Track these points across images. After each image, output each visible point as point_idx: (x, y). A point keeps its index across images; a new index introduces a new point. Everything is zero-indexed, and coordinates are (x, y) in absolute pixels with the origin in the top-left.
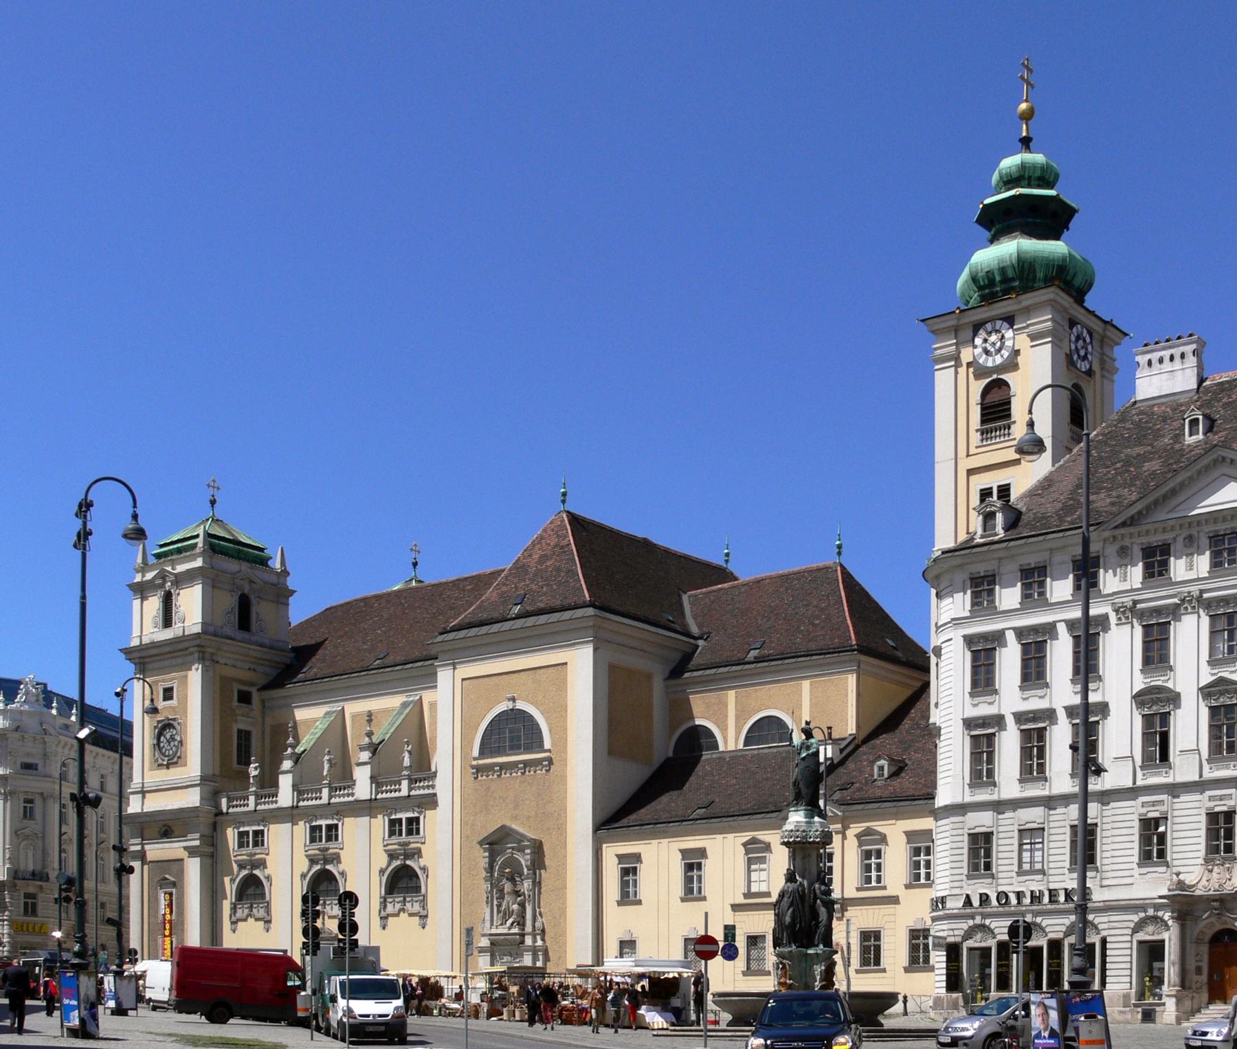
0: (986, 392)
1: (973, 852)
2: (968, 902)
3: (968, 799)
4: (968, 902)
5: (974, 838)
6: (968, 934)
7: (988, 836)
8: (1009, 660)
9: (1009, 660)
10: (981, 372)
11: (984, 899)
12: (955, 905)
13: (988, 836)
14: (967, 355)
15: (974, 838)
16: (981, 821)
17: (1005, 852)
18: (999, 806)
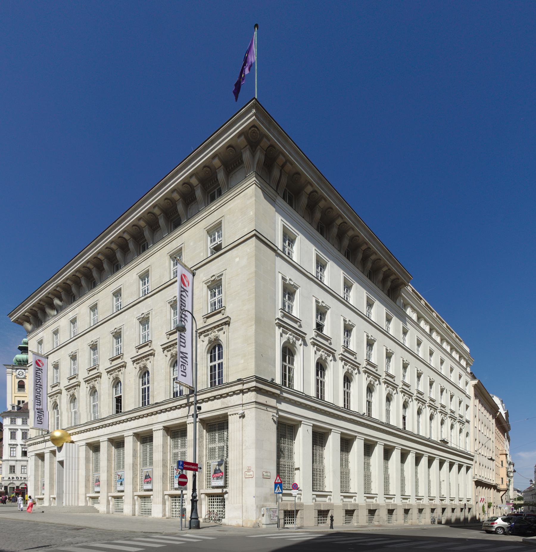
0: (19, 382)
1: (11, 469)
2: (9, 478)
3: (9, 459)
4: (9, 478)
5: (11, 466)
6: (9, 484)
7: (14, 466)
8: (19, 434)
9: (19, 434)
10: (18, 378)
11: (13, 478)
12: (7, 479)
13: (14, 466)
14: (14, 374)
15: (11, 466)
16: (13, 463)
17: (18, 469)
18: (17, 461)
